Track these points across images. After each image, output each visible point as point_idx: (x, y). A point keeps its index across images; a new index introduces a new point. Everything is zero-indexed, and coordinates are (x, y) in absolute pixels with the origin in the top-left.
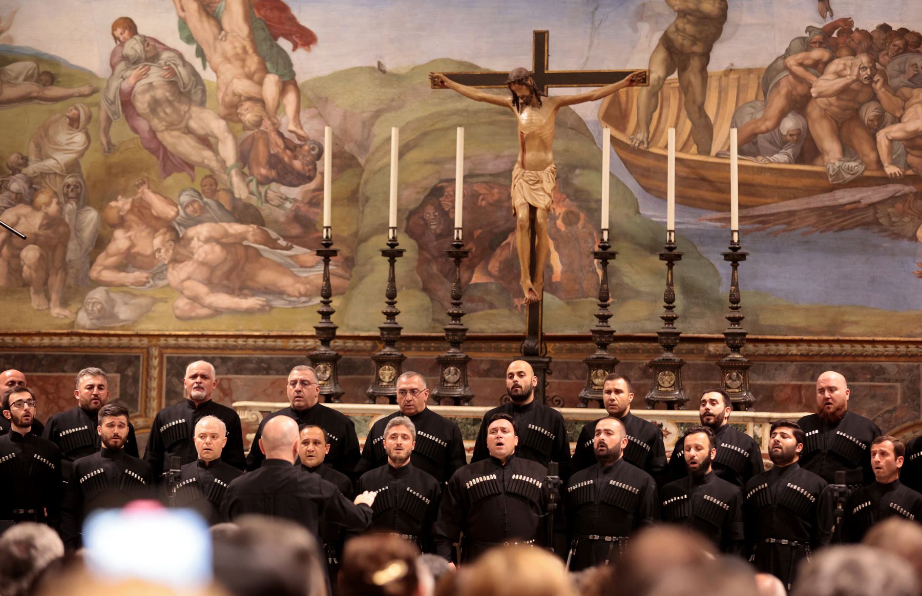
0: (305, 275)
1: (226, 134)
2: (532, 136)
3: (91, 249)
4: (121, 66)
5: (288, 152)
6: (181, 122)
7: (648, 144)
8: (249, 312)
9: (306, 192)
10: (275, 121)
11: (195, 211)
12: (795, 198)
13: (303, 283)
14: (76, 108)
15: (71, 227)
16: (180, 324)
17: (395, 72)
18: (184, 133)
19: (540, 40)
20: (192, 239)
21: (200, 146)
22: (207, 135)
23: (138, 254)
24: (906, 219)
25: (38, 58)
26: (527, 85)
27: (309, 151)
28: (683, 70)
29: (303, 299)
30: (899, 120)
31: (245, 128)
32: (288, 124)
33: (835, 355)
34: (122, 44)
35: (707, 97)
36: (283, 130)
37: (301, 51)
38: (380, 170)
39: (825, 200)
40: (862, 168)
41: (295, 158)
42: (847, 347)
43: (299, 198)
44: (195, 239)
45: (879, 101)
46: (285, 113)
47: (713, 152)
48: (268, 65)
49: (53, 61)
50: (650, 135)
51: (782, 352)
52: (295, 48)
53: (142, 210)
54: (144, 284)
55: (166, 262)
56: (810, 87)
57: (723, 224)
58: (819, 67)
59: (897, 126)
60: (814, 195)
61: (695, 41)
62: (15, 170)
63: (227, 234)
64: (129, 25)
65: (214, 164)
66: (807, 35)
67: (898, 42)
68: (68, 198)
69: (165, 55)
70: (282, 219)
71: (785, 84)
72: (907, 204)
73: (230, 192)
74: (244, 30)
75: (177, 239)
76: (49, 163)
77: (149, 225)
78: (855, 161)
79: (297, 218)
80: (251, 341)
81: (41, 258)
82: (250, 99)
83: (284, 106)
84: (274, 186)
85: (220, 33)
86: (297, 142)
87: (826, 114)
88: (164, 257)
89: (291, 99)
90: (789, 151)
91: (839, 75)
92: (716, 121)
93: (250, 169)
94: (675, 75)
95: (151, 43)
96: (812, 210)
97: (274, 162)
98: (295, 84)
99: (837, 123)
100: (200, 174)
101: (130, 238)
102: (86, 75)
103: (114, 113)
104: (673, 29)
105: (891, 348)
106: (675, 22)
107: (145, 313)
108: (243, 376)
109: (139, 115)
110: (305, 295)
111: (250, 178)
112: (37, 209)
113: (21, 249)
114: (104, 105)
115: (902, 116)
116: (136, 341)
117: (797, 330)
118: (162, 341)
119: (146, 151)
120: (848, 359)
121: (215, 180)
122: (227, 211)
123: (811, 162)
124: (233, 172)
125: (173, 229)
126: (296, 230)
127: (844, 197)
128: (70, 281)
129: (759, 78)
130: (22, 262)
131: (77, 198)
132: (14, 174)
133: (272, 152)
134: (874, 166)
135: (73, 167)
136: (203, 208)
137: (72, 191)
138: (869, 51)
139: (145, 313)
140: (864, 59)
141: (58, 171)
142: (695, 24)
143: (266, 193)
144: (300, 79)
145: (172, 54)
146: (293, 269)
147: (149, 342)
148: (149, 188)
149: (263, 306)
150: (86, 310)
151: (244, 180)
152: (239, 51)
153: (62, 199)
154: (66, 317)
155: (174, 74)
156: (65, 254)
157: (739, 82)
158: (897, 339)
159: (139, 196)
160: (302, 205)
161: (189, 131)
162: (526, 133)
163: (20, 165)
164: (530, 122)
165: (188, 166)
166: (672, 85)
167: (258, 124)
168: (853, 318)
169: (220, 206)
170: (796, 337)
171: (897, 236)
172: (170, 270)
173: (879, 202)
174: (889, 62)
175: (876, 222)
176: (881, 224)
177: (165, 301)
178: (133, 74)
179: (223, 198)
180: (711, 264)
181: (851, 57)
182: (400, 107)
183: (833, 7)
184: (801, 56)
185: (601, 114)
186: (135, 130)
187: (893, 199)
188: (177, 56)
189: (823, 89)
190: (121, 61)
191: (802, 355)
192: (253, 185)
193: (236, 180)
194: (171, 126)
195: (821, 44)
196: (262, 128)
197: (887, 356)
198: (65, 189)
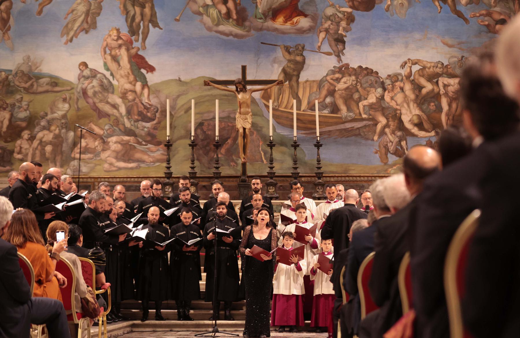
0: (152, 155)
1: (122, 104)
2: (244, 102)
3: (71, 146)
4: (82, 79)
5: (145, 110)
6: (105, 99)
7: (278, 107)
8: (132, 169)
9: (152, 125)
10: (140, 99)
11: (110, 132)
12: (331, 126)
13: (152, 158)
14: (65, 95)
15: (64, 138)
16: (107, 174)
17: (185, 81)
18: (106, 103)
19: (244, 68)
20: (110, 142)
21: (112, 108)
22: (115, 104)
23: (89, 148)
24: (370, 133)
25: (51, 77)
26: (242, 84)
27: (153, 110)
28: (290, 81)
29: (152, 164)
30: (366, 99)
31: (129, 102)
32: (145, 100)
33: (347, 181)
34: (83, 71)
35: (299, 90)
36: (143, 102)
37: (150, 74)
38: (180, 116)
39: (342, 126)
40: (354, 115)
41: (148, 112)
42: (351, 178)
43: (150, 127)
44: (111, 142)
45: (359, 92)
46: (144, 96)
47: (302, 110)
48: (137, 79)
49: (57, 78)
50: (279, 104)
51: (328, 181)
52: (147, 72)
53: (91, 132)
54: (92, 159)
55: (100, 151)
56: (335, 87)
57: (306, 135)
58: (338, 80)
59: (366, 101)
60: (338, 125)
61: (294, 70)
62: (43, 118)
63: (123, 140)
64: (85, 65)
65: (118, 115)
66: (334, 69)
67: (365, 72)
68: (63, 128)
69: (99, 75)
70: (143, 134)
71: (326, 86)
72: (370, 128)
73: (124, 125)
74: (128, 66)
75: (104, 142)
76: (55, 115)
77: (93, 137)
78: (352, 113)
79: (149, 134)
80: (133, 179)
81: (53, 150)
82: (131, 91)
83: (144, 94)
84: (140, 122)
85: (119, 67)
86: (149, 106)
87: (341, 97)
88: (99, 149)
89: (146, 91)
90: (329, 109)
91: (345, 83)
92: (302, 99)
93: (131, 116)
94: (287, 83)
95: (93, 71)
96: (337, 130)
97: (140, 114)
98: (147, 85)
99: (345, 100)
100: (112, 118)
101: (86, 142)
102: (69, 83)
103: (80, 97)
104: (286, 66)
105: (366, 178)
106: (287, 63)
107: (92, 169)
108: (130, 192)
109: (89, 97)
110: (153, 162)
111: (131, 120)
112: (51, 132)
113: (45, 147)
114: (76, 94)
115: (367, 97)
116: (89, 180)
117: (333, 172)
118: (99, 180)
119: (92, 110)
120: (351, 182)
121: (118, 120)
122: (122, 131)
123: (336, 113)
124: (125, 118)
125: (102, 139)
126: (149, 139)
127: (348, 125)
128: (64, 158)
129: (317, 84)
130: (46, 152)
131: (66, 128)
132: (42, 119)
133: (139, 110)
134: (358, 115)
135: (64, 116)
136: (114, 131)
137: (64, 125)
138: (355, 75)
139: (92, 169)
140: (353, 78)
141: (59, 118)
142: (294, 65)
143: (137, 125)
144: (149, 84)
145: (101, 75)
146: (148, 153)
147: (94, 180)
148: (93, 124)
149: (137, 166)
150: (70, 169)
151: (129, 120)
152: (127, 74)
153: (60, 128)
154: (62, 171)
155: (102, 82)
156: (62, 148)
157: (310, 85)
158: (368, 175)
159: (89, 126)
160: (151, 129)
161: (108, 103)
162: (241, 101)
163: (44, 116)
164: (243, 97)
165: (108, 115)
166: (287, 86)
167: (134, 100)
168: (353, 168)
169: (120, 130)
170: (333, 175)
171: (367, 139)
172: (102, 154)
173: (360, 127)
174: (362, 79)
175: (360, 134)
176: (361, 135)
177: (100, 165)
178: (86, 82)
179: (121, 127)
180: (302, 149)
181: (349, 77)
182: (187, 94)
183: (342, 59)
184: (332, 76)
185: (261, 96)
186: (88, 103)
187: (365, 126)
188: (103, 76)
189: (340, 88)
190: (82, 78)
191: (335, 181)
192: (132, 123)
193: (126, 120)
194: (101, 101)
195: (339, 72)
196: (135, 102)
197: (365, 181)
198: (62, 125)
